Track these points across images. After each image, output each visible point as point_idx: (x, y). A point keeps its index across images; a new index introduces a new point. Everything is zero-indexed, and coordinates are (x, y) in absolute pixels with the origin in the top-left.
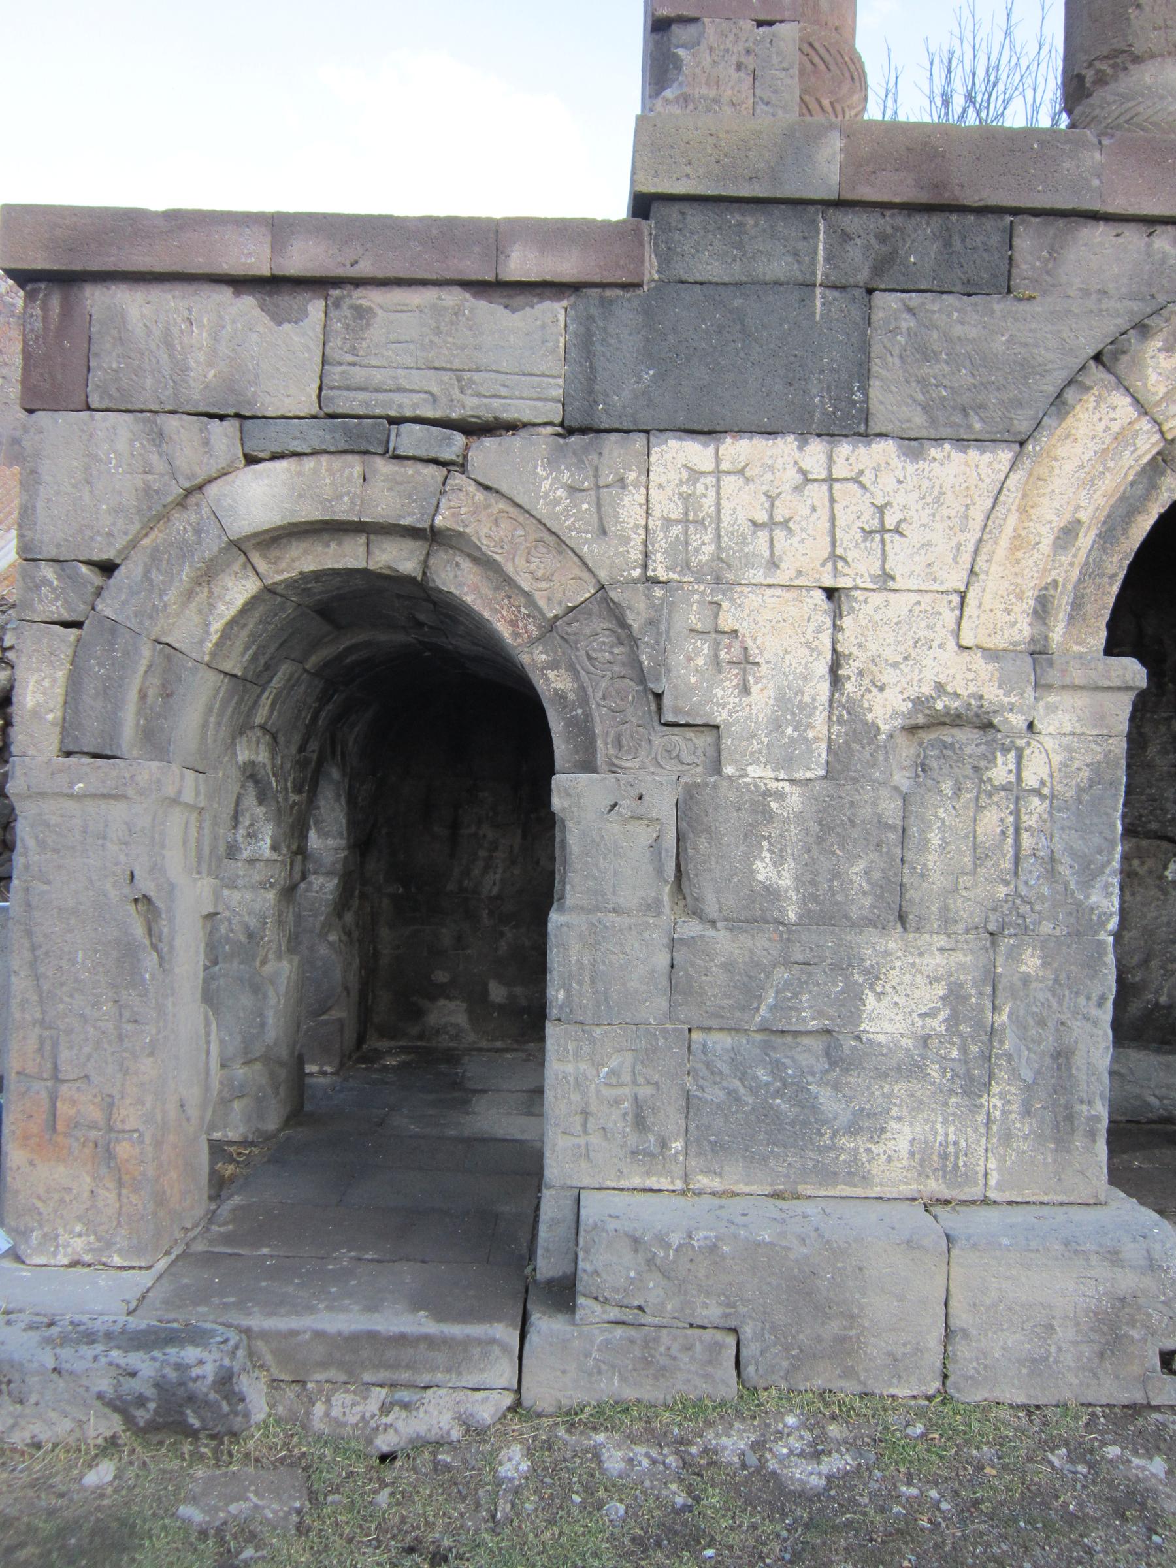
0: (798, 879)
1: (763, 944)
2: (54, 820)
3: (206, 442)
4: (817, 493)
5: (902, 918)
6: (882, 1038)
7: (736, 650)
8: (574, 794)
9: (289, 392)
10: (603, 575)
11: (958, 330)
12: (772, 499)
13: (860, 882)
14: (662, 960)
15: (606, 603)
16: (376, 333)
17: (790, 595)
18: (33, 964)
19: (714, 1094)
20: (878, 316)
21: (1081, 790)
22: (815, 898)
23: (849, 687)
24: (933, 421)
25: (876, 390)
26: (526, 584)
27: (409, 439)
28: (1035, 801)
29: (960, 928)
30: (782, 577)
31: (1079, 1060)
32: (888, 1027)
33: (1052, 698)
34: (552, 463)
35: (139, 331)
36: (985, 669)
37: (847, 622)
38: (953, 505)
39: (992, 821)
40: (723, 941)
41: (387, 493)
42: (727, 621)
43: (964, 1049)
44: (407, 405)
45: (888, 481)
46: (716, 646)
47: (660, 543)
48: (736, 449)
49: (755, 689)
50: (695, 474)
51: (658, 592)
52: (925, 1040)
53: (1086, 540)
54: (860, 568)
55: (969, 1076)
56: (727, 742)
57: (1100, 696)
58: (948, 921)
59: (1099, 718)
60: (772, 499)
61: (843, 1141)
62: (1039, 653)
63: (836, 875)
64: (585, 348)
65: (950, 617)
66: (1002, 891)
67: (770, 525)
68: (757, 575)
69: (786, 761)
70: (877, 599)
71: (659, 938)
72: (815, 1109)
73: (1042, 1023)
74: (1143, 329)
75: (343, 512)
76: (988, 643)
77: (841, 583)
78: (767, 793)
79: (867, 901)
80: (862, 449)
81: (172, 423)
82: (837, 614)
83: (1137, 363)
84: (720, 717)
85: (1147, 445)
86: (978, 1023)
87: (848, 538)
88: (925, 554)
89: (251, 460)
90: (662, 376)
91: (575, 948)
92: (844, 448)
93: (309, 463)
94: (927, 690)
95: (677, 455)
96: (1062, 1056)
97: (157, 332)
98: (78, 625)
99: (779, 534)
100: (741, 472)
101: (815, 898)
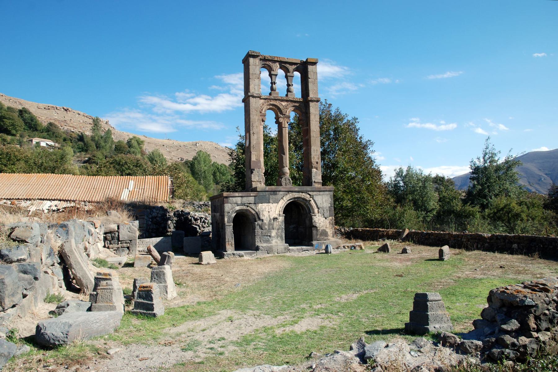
9: (239, 202)
15: (257, 213)
41: (245, 208)
64: (255, 199)
88: (273, 209)
95: (260, 205)
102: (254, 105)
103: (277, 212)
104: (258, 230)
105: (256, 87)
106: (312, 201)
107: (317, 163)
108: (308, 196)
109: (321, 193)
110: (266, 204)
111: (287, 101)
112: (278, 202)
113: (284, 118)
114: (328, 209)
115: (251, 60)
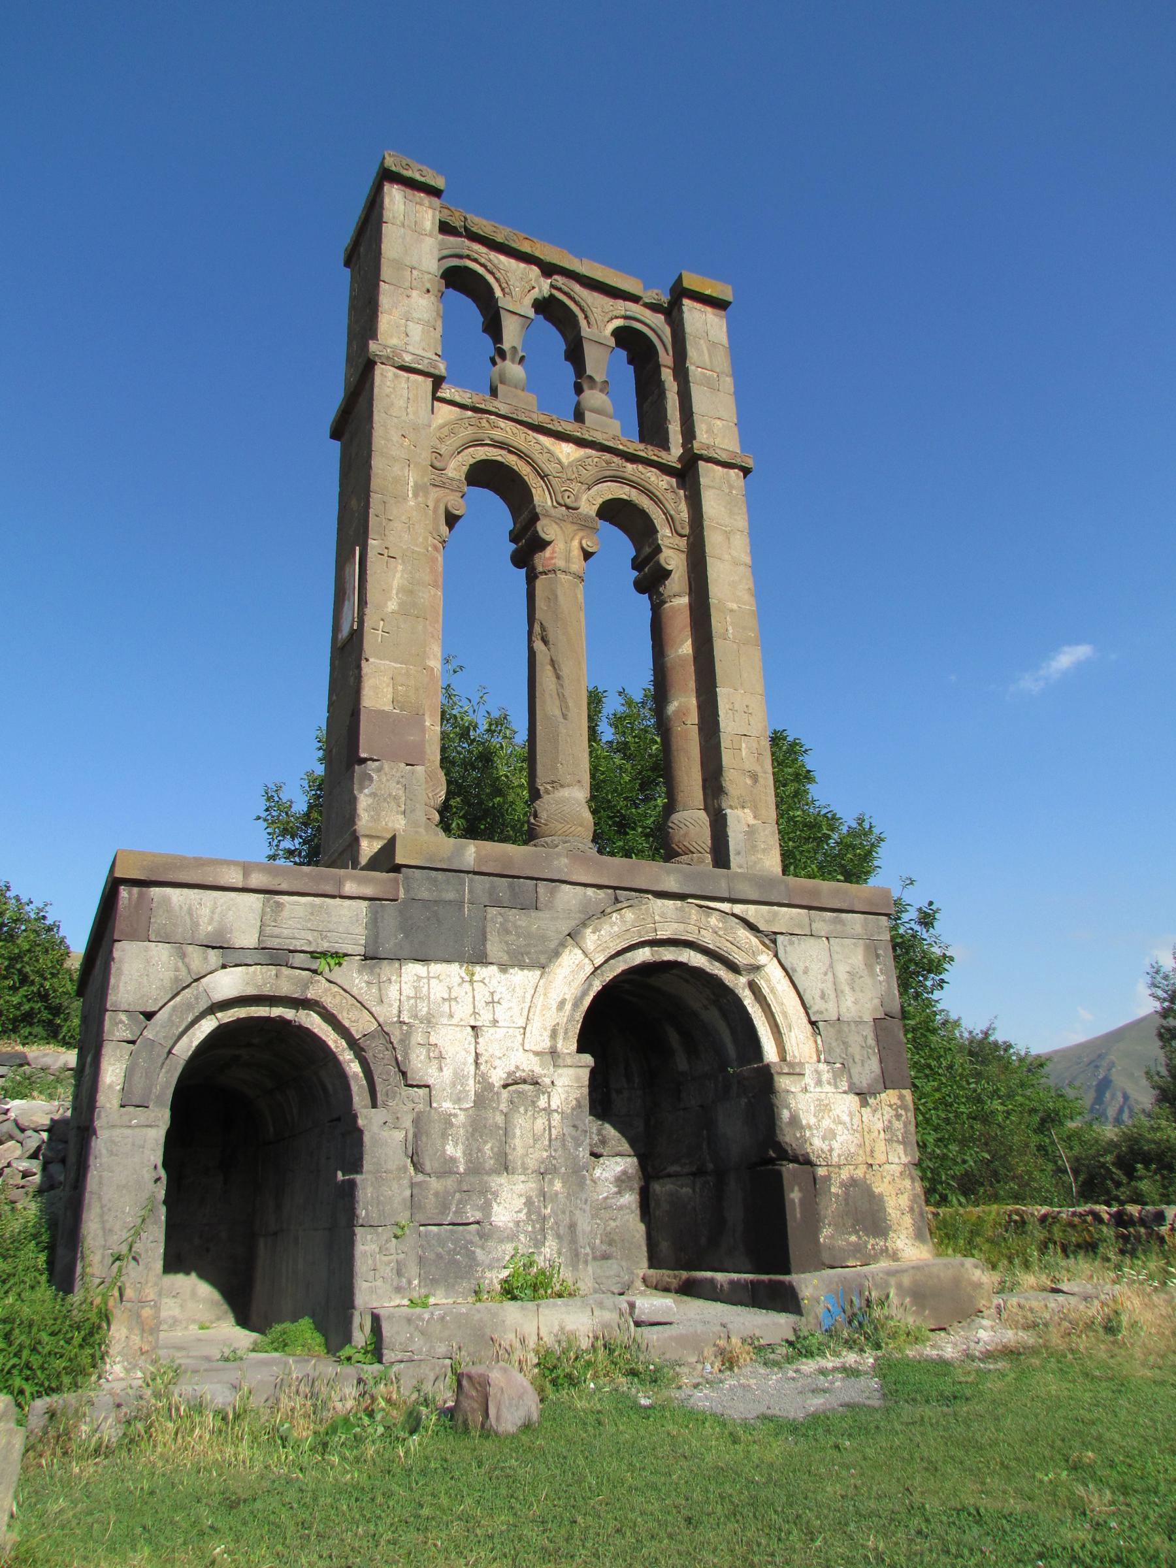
0: (464, 1153)
1: (450, 1183)
2: (117, 1139)
3: (206, 958)
4: (467, 986)
5: (506, 1169)
6: (500, 1224)
7: (437, 1054)
8: (369, 1120)
9: (247, 938)
10: (381, 1020)
11: (519, 923)
12: (450, 989)
13: (489, 1152)
14: (408, 1193)
16: (285, 913)
17: (458, 1029)
18: (102, 1216)
19: (430, 1255)
20: (489, 916)
21: (573, 1109)
22: (471, 1161)
23: (482, 1067)
24: (511, 958)
25: (489, 946)
26: (346, 1023)
27: (299, 959)
28: (556, 1114)
29: (530, 1171)
30: (455, 1021)
31: (579, 1229)
32: (503, 1219)
33: (560, 1071)
34: (360, 972)
35: (177, 908)
36: (535, 1059)
37: (480, 1040)
38: (519, 992)
39: (540, 1123)
40: (434, 1184)
41: (285, 982)
42: (433, 1040)
43: (533, 1227)
44: (298, 945)
45: (494, 982)
46: (428, 1051)
47: (406, 1006)
48: (436, 968)
49: (445, 1069)
50: (420, 978)
51: (405, 1028)
52: (517, 1223)
53: (568, 1007)
54: (485, 1018)
55: (536, 1239)
56: (434, 1092)
57: (578, 1070)
58: (525, 1168)
59: (578, 1079)
60: (450, 989)
61: (488, 1274)
62: (553, 1052)
63: (479, 1150)
64: (374, 923)
65: (520, 1038)
66: (545, 1154)
67: (449, 1000)
68: (445, 1020)
69: (458, 1100)
70: (492, 1030)
71: (406, 1182)
72: (474, 1259)
73: (564, 1212)
74: (584, 925)
75: (267, 991)
76: (534, 1049)
77: (477, 1024)
78: (450, 1115)
79: (492, 1162)
80: (484, 969)
81: (190, 948)
82: (477, 1036)
83: (584, 938)
84: (431, 1082)
85: (589, 969)
86: (539, 1214)
87: (480, 1005)
88: (510, 1012)
89: (224, 967)
90: (406, 936)
91: (369, 1190)
92: (478, 969)
93: (252, 969)
94: (513, 1068)
95: (413, 970)
96: (572, 1226)
97: (185, 908)
98: (133, 1042)
99: (453, 1003)
100: (438, 977)
101: (471, 1161)
102: (394, 412)
103: (539, 1039)
104: (384, 1180)
105: (416, 331)
106: (773, 971)
107: (755, 778)
108: (743, 934)
109: (822, 922)
110: (454, 971)
111: (581, 443)
112: (538, 957)
113: (559, 521)
114: (868, 1031)
115: (395, 198)
